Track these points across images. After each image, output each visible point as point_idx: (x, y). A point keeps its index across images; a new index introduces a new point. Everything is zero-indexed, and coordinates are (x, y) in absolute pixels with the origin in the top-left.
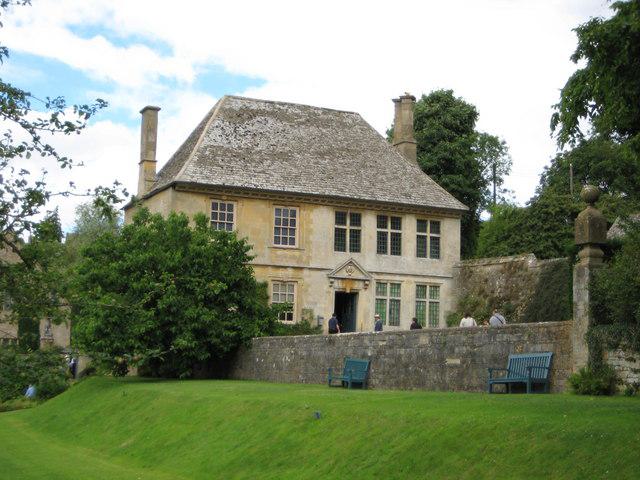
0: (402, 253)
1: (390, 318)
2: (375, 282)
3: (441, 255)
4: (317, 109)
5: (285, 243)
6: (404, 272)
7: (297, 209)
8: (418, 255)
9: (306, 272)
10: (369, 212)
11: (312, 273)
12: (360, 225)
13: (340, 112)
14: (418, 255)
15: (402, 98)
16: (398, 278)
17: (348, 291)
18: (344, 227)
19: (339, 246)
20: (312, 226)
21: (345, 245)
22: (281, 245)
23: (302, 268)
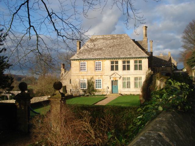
12: (118, 64)
16: (129, 76)
19: (112, 69)
23: (102, 76)
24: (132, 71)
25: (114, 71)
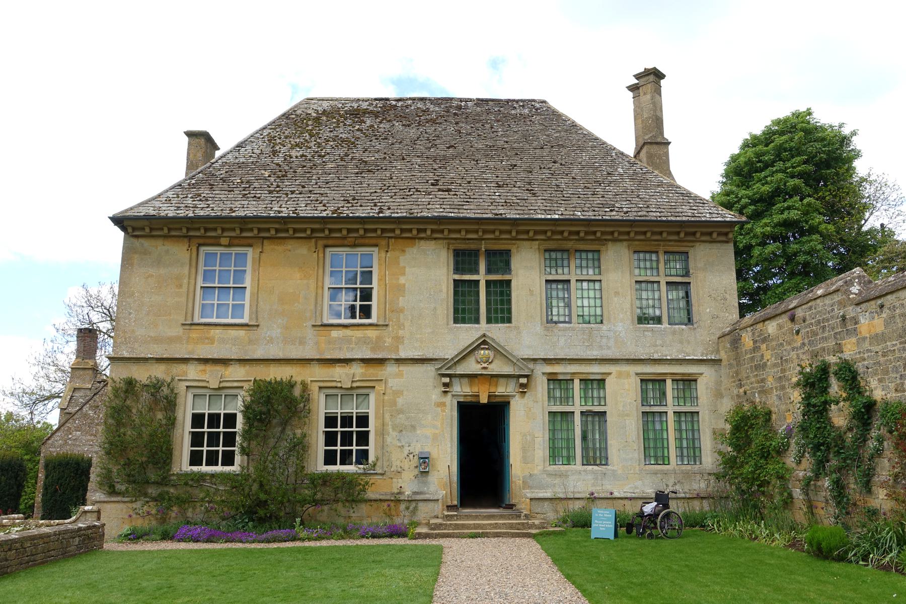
1: (585, 449)
2: (545, 379)
3: (695, 320)
4: (467, 100)
6: (609, 354)
9: (391, 369)
11: (406, 369)
13: (508, 101)
15: (638, 77)
17: (484, 400)
18: (474, 277)
20: (402, 280)
21: (478, 310)
23: (381, 362)
24: (620, 327)
25: (483, 327)
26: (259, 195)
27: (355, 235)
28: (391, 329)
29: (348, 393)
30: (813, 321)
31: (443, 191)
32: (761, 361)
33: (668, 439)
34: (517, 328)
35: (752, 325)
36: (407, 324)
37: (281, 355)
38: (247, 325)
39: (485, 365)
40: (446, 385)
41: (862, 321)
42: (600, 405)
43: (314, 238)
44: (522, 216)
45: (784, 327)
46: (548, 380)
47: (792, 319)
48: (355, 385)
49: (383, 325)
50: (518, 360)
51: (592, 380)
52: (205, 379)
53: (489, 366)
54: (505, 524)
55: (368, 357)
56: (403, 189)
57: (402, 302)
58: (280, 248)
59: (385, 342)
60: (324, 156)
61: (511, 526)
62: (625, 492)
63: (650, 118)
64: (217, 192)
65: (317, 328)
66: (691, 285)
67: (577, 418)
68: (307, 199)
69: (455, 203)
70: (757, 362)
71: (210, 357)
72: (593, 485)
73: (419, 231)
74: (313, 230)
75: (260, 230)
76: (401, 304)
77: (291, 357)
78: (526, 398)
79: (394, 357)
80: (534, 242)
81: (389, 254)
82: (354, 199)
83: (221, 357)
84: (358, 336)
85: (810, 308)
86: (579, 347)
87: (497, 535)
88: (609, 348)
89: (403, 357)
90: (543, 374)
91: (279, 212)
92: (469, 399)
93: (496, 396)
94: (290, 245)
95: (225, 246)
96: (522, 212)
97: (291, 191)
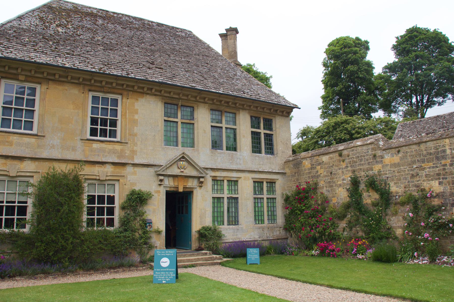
0: (238, 150)
1: (229, 217)
2: (210, 179)
3: (275, 153)
5: (104, 133)
7: (119, 97)
8: (254, 152)
9: (129, 169)
10: (202, 105)
11: (137, 169)
14: (254, 152)
15: (227, 30)
16: (234, 175)
17: (181, 190)
20: (136, 117)
22: (98, 138)
26: (46, 52)
27: (110, 86)
28: (129, 146)
29: (102, 182)
30: (354, 156)
31: (159, 68)
32: (316, 174)
33: (263, 211)
34: (198, 150)
35: (311, 157)
36: (139, 143)
37: (60, 157)
38: (36, 135)
39: (182, 170)
40: (161, 181)
41: (386, 157)
42: (235, 194)
43: (83, 84)
44: (204, 89)
45: (334, 159)
46: (212, 180)
47: (340, 155)
48: (108, 178)
49: (125, 143)
50: (200, 168)
51: (232, 181)
52: (6, 169)
53: (185, 171)
54: (202, 258)
55: (116, 161)
56: (135, 64)
57: (136, 130)
58: (60, 87)
59: (126, 153)
60: (79, 36)
61: (206, 260)
62: (247, 238)
63: (233, 51)
64: (14, 44)
65: (84, 141)
66: (274, 135)
67: (226, 201)
68: (78, 59)
69: (168, 76)
70: (313, 174)
71: (10, 155)
72: (233, 235)
73: (148, 89)
74: (84, 79)
75: (48, 74)
76: (135, 131)
77: (68, 159)
78: (202, 189)
79: (132, 163)
80: (206, 104)
81: (129, 101)
82: (108, 64)
83: (18, 155)
84: (109, 148)
85: (353, 150)
86: (227, 163)
87: (202, 265)
88: (240, 164)
89: (138, 163)
90: (211, 176)
91: (65, 64)
92: (172, 189)
93: (187, 188)
94: (67, 87)
95: (22, 81)
96: (203, 87)
97: (66, 53)
